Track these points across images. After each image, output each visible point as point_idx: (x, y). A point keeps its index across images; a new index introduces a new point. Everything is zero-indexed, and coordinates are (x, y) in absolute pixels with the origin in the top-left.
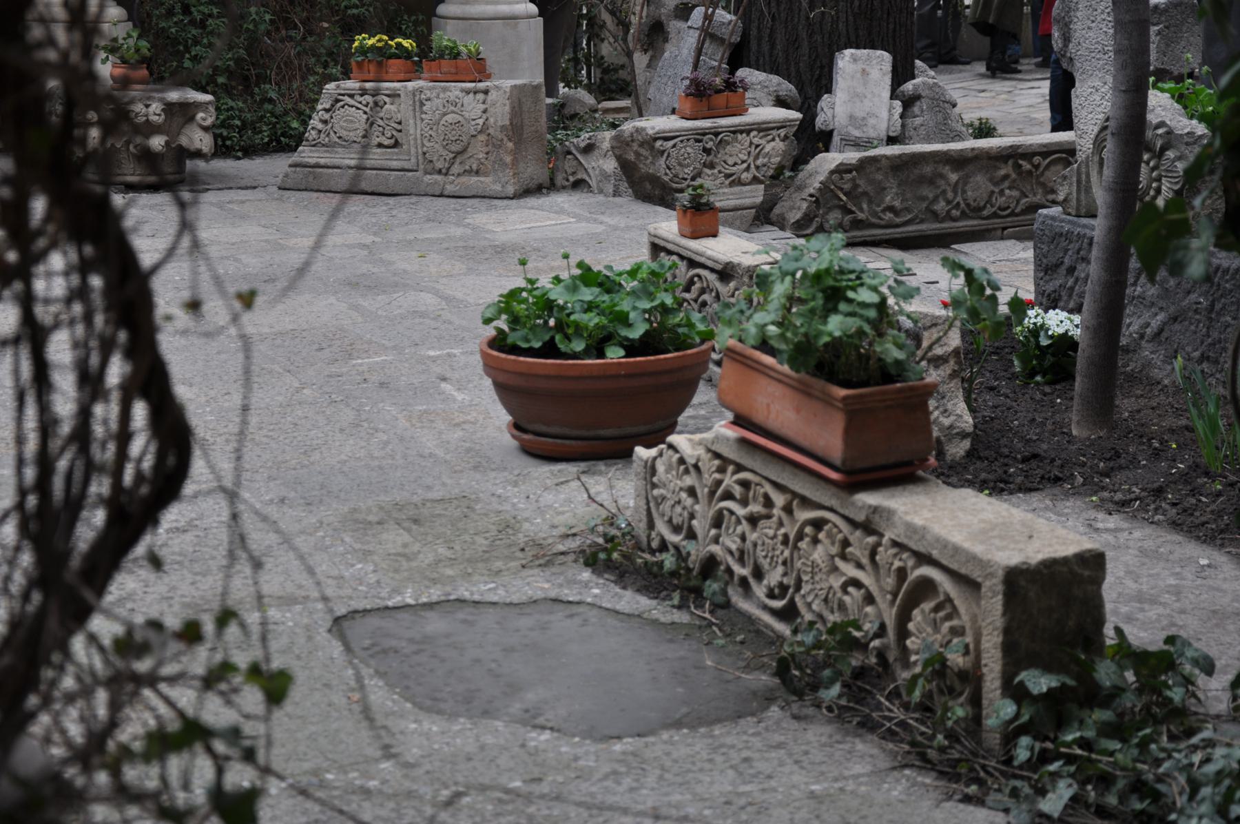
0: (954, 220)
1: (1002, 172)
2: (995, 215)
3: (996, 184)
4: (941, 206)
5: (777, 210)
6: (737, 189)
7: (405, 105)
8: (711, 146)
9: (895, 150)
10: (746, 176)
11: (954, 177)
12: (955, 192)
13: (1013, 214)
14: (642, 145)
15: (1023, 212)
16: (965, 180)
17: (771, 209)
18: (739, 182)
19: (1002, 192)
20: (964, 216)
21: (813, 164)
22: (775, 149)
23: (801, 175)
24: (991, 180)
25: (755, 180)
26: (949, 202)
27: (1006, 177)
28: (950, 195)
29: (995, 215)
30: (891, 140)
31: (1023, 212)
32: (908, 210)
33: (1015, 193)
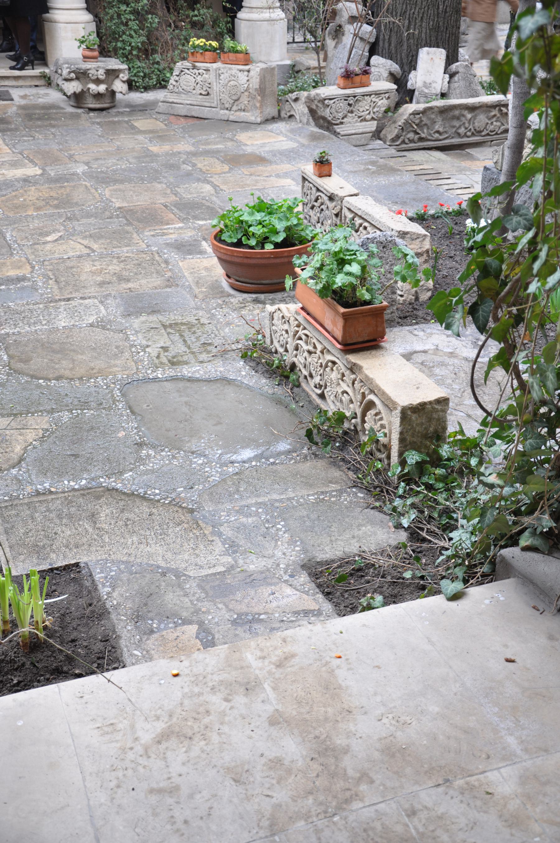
0: (468, 137)
1: (493, 114)
2: (488, 135)
3: (489, 119)
4: (462, 131)
5: (383, 132)
6: (364, 123)
7: (212, 75)
8: (352, 102)
9: (441, 103)
10: (368, 117)
11: (469, 116)
12: (469, 123)
13: (497, 134)
14: (319, 101)
15: (502, 133)
16: (474, 117)
17: (381, 131)
18: (365, 120)
19: (492, 123)
20: (473, 134)
21: (401, 110)
22: (383, 103)
23: (396, 115)
24: (487, 117)
25: (373, 119)
26: (466, 128)
27: (495, 116)
28: (467, 125)
29: (488, 135)
30: (443, 95)
31: (502, 133)
32: (446, 132)
33: (498, 124)
